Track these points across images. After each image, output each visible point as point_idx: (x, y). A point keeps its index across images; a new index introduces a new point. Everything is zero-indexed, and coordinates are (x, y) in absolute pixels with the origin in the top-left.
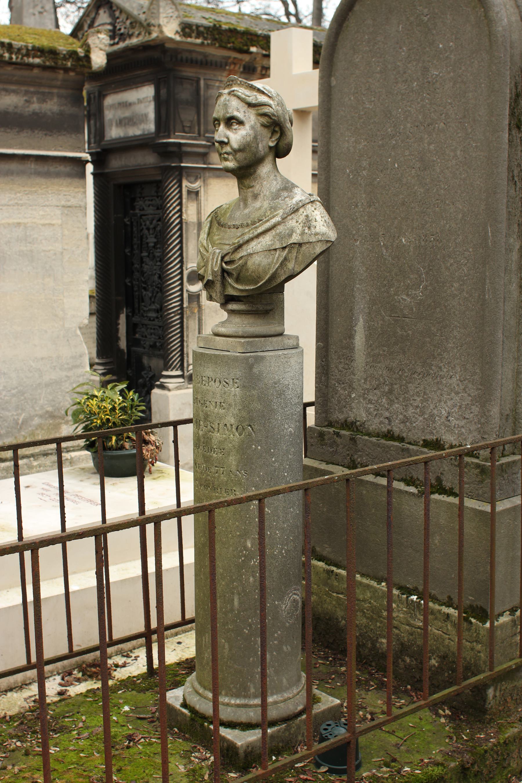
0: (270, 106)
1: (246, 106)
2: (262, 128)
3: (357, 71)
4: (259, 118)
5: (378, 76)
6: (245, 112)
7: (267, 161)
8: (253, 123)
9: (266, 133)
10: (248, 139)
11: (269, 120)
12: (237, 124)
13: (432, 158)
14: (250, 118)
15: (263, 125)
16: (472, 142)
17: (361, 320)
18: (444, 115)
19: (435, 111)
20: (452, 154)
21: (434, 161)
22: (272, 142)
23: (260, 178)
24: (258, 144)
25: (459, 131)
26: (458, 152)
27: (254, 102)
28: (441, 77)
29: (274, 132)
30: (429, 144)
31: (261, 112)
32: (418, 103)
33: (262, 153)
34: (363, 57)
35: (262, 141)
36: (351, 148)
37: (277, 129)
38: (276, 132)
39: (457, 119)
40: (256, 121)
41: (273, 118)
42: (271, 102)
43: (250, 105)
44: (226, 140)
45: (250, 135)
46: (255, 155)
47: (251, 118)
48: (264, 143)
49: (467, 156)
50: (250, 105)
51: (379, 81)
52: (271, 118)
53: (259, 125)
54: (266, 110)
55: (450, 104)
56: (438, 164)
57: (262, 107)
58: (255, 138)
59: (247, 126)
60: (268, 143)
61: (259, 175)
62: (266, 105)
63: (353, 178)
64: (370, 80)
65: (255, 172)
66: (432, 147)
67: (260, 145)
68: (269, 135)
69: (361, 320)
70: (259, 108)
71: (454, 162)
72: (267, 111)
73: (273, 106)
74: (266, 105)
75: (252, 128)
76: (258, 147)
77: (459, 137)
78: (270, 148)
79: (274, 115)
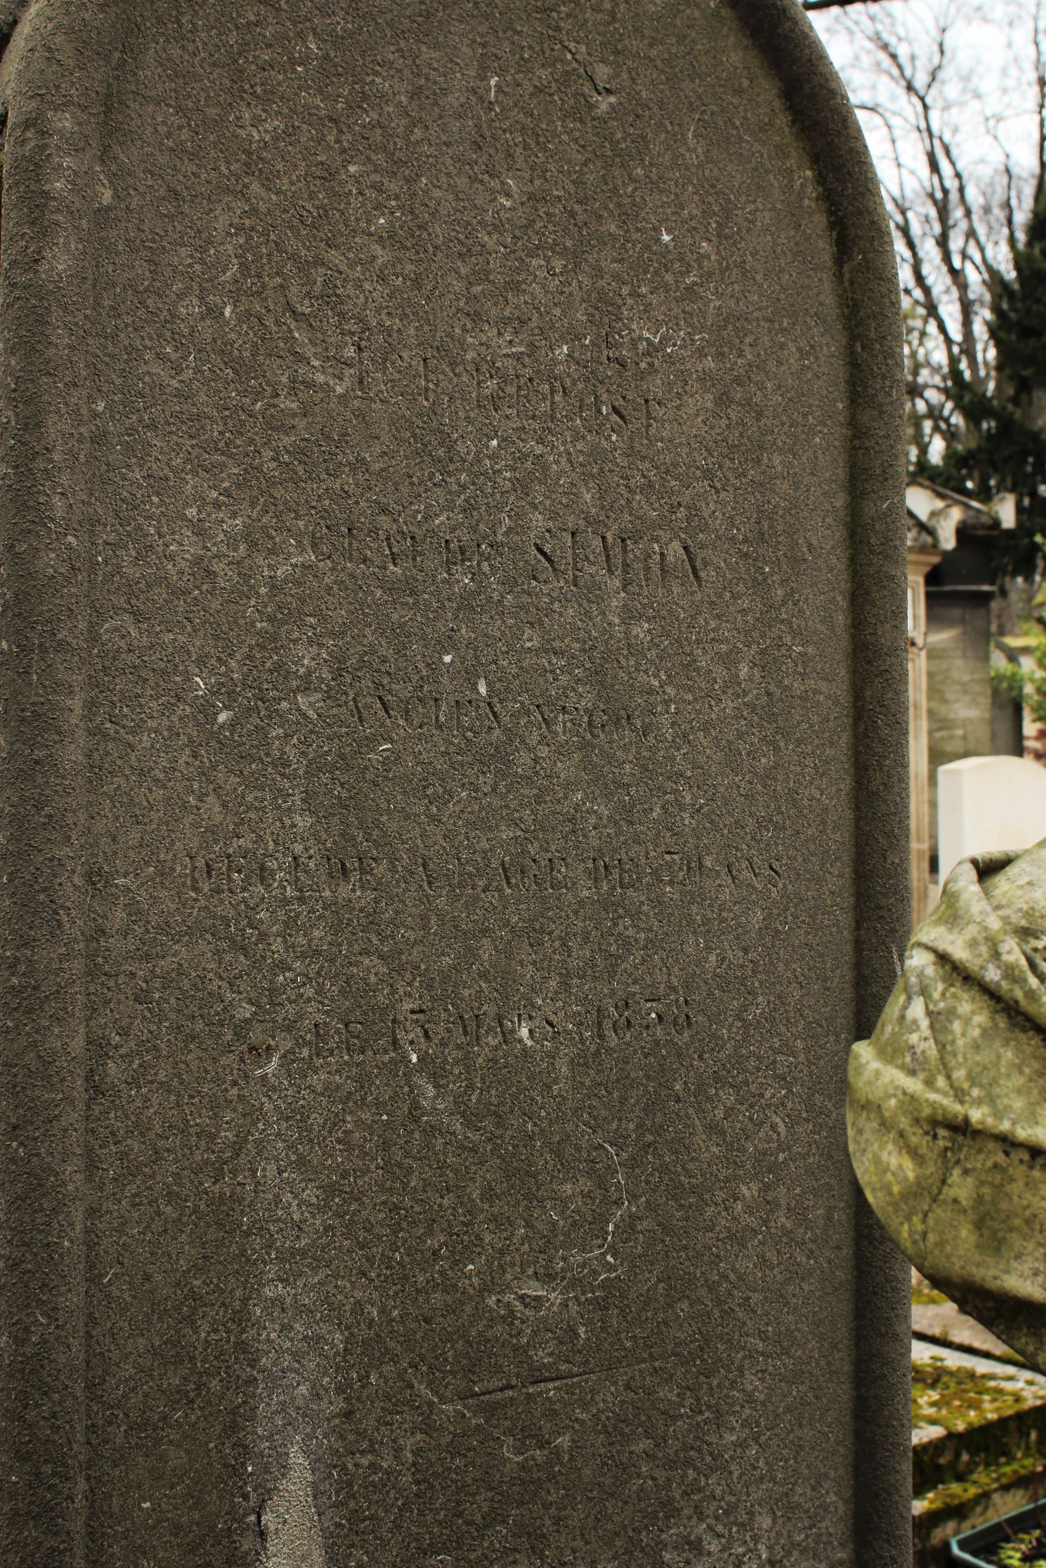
3: (256, 188)
5: (382, 255)
13: (642, 677)
16: (788, 639)
17: (297, 1458)
18: (682, 513)
19: (651, 485)
20: (720, 672)
21: (651, 691)
25: (741, 588)
26: (744, 671)
28: (669, 359)
30: (629, 616)
32: (577, 437)
34: (292, 131)
36: (217, 567)
39: (733, 538)
49: (772, 688)
51: (382, 278)
55: (708, 474)
56: (666, 703)
63: (233, 725)
64: (334, 257)
66: (640, 630)
69: (297, 1458)
71: (729, 705)
77: (743, 612)
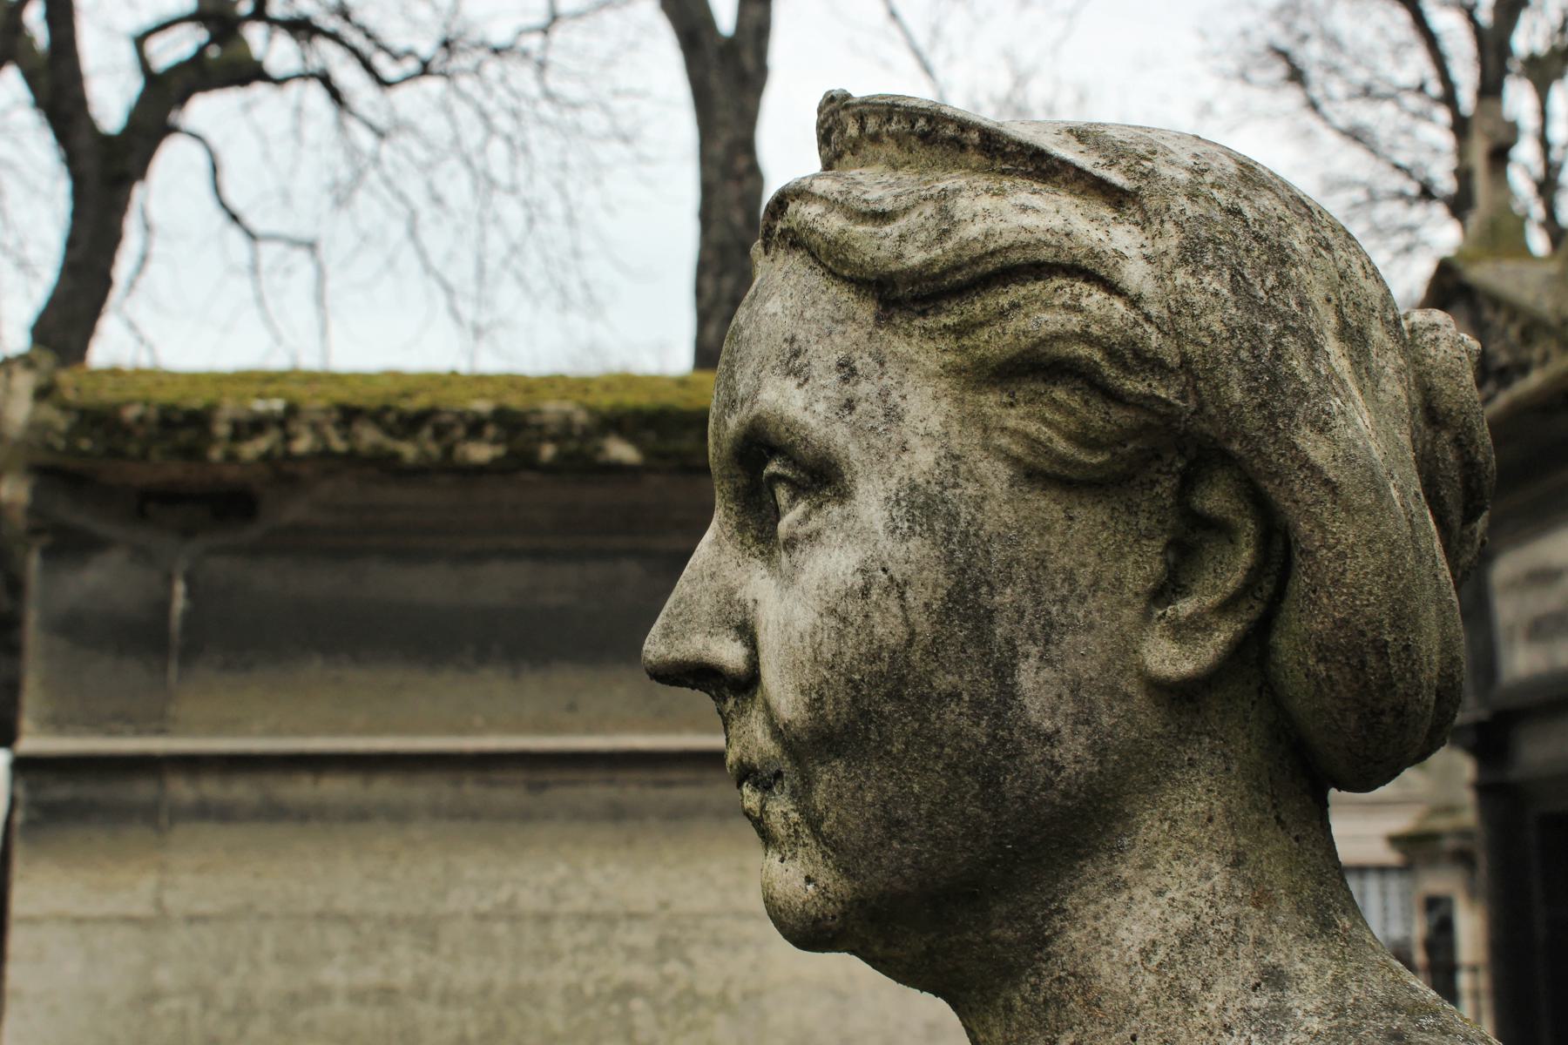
0: (1091, 272)
1: (866, 311)
2: (1043, 504)
4: (990, 401)
6: (847, 370)
7: (1150, 826)
8: (924, 458)
9: (1092, 549)
10: (888, 627)
11: (1097, 416)
12: (798, 490)
14: (893, 415)
15: (1037, 473)
22: (1182, 631)
23: (1092, 1004)
24: (1003, 671)
27: (915, 257)
29: (1189, 542)
31: (996, 342)
33: (1073, 750)
35: (1049, 632)
37: (1215, 500)
38: (1219, 528)
40: (967, 441)
41: (1134, 386)
42: (1121, 239)
43: (897, 295)
44: (730, 654)
45: (899, 587)
46: (990, 779)
47: (904, 422)
48: (1085, 654)
50: (897, 295)
52: (1113, 396)
53: (997, 475)
54: (1045, 314)
57: (1016, 292)
58: (965, 604)
59: (871, 502)
60: (1127, 648)
61: (1084, 980)
62: (1039, 270)
65: (1039, 942)
67: (1028, 676)
68: (1143, 566)
70: (976, 308)
72: (1052, 320)
73: (1135, 275)
74: (1039, 270)
75: (921, 508)
76: (1008, 692)
78: (1178, 696)
79: (1150, 363)
